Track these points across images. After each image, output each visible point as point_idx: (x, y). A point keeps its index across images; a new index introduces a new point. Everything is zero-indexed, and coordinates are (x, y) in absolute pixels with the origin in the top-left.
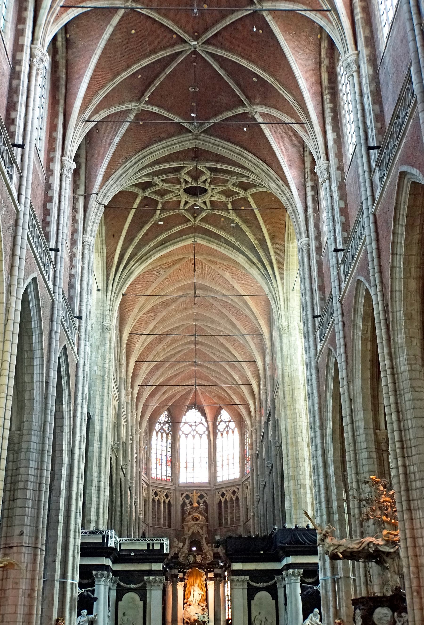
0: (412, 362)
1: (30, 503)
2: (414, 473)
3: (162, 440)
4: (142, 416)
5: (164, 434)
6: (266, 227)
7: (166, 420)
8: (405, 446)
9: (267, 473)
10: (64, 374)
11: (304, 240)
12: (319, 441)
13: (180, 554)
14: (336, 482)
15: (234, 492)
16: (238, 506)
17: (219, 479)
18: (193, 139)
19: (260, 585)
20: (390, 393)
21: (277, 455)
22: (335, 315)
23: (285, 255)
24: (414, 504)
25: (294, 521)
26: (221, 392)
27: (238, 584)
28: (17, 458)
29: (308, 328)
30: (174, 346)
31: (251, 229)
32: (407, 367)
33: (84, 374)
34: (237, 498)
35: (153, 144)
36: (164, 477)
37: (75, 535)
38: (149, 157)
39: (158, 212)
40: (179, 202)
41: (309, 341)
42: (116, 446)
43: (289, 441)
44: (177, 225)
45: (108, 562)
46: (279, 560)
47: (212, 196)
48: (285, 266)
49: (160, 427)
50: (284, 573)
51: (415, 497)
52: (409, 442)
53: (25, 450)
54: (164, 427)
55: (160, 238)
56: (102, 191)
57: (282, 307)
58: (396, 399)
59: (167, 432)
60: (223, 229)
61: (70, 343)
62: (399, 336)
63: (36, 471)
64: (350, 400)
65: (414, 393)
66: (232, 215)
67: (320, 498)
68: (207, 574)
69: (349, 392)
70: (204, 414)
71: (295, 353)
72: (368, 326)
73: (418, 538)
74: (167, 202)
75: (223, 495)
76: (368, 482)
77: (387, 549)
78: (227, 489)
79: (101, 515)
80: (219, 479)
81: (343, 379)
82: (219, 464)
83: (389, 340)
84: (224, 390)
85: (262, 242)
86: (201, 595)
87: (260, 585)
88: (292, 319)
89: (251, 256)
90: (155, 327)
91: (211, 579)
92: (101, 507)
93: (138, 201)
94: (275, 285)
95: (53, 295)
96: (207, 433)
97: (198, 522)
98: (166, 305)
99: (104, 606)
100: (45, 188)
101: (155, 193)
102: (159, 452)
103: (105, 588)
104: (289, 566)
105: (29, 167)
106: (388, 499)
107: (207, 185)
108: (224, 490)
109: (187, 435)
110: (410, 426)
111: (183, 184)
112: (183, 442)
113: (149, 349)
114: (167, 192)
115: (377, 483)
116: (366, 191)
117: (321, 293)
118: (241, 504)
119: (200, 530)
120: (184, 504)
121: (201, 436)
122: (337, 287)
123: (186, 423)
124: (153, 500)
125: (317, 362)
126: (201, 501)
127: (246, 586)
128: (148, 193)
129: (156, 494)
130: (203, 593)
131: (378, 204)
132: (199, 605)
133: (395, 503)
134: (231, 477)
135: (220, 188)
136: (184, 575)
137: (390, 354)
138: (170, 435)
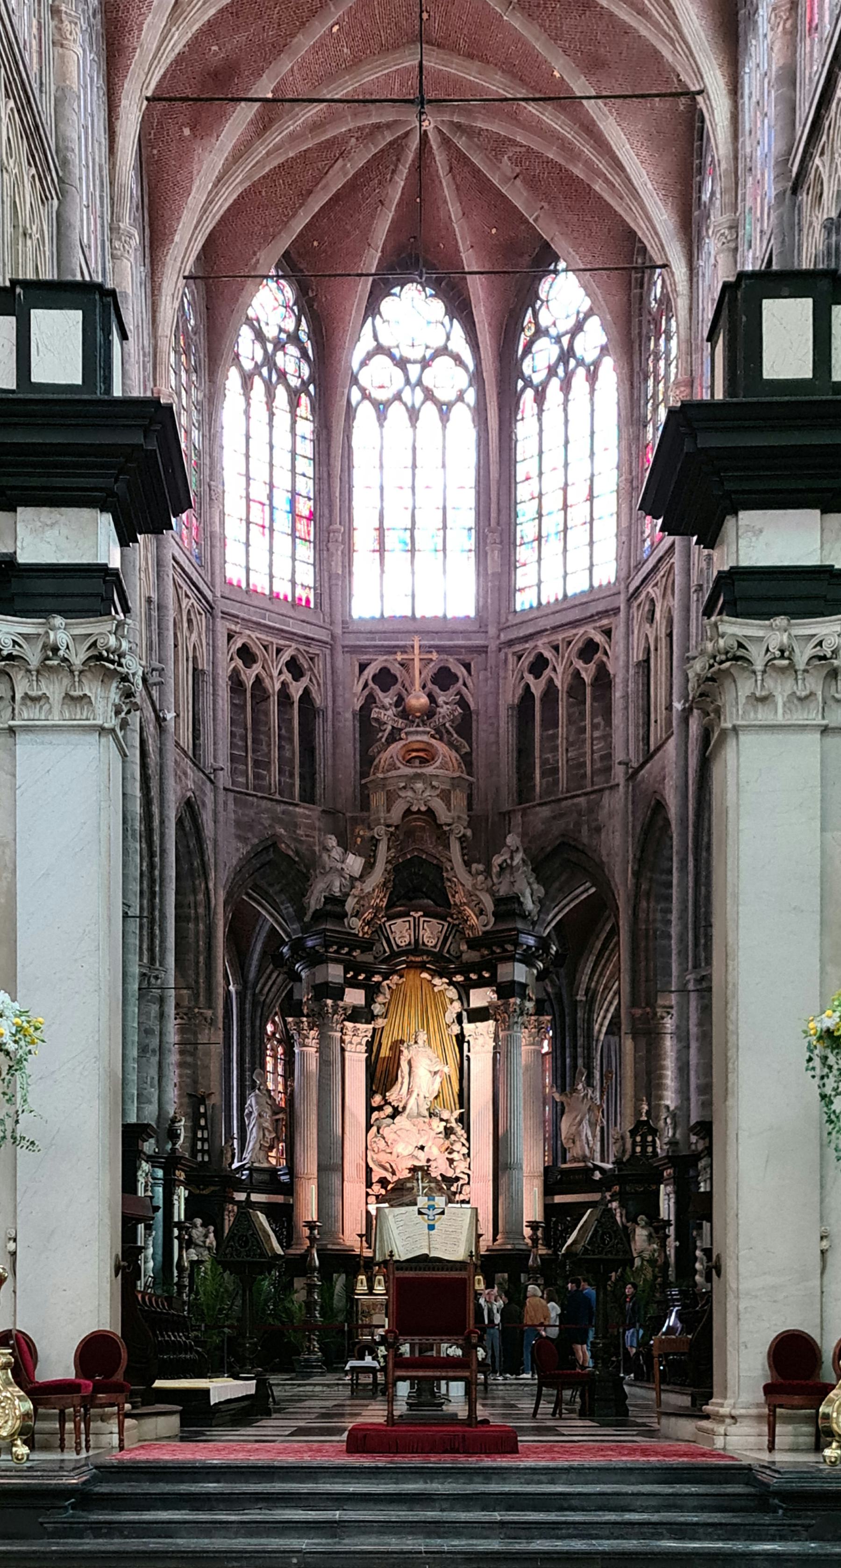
3: (272, 415)
15: (589, 650)
16: (607, 713)
34: (603, 679)
54: (280, 358)
59: (294, 382)
68: (464, 997)
78: (559, 637)
86: (438, 1079)
96: (471, 396)
102: (260, 472)
120: (371, 699)
121: (444, 410)
130: (446, 1069)
132: (431, 1115)
134: (578, 585)
138: (304, 400)
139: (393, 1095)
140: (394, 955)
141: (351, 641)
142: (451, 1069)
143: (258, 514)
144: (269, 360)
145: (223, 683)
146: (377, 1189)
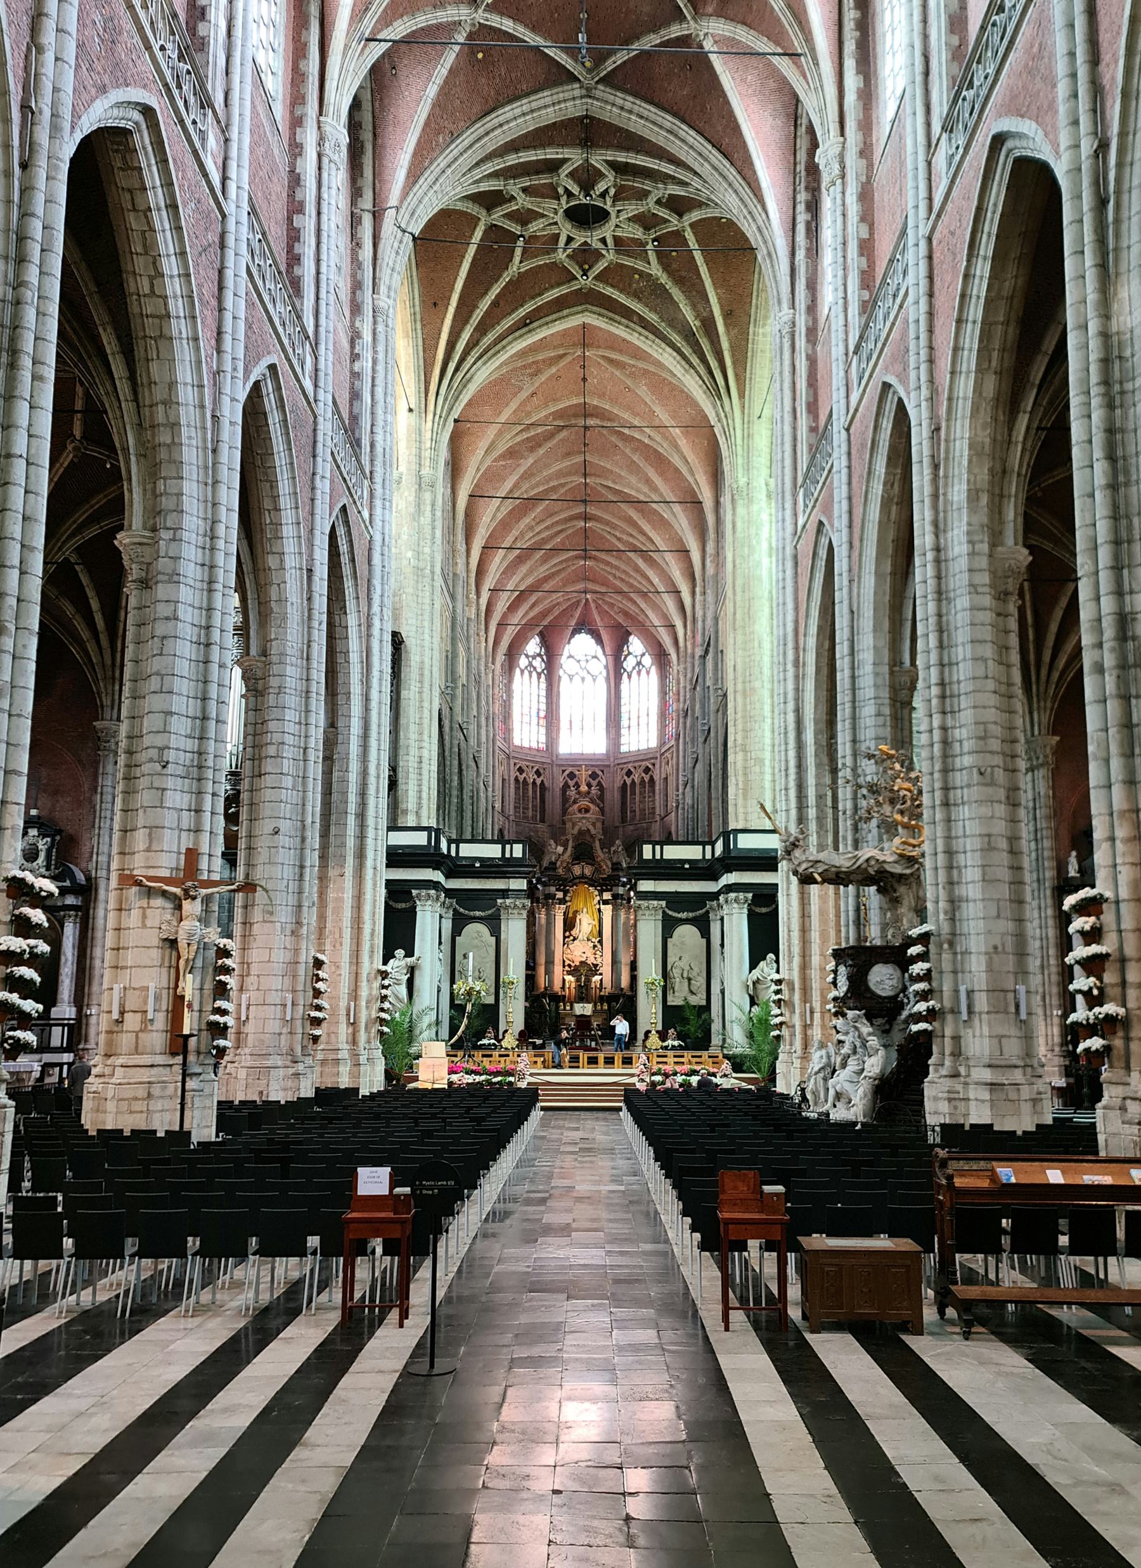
0: (976, 538)
1: (288, 782)
2: (961, 741)
4: (496, 643)
5: (534, 674)
6: (717, 294)
7: (538, 651)
8: (948, 693)
9: (701, 740)
10: (345, 559)
11: (786, 313)
12: (790, 686)
13: (559, 863)
14: (816, 755)
15: (647, 770)
17: (624, 749)
18: (582, 97)
19: (683, 915)
20: (930, 597)
21: (718, 711)
22: (835, 455)
23: (750, 349)
24: (955, 795)
25: (741, 817)
26: (629, 604)
27: (647, 913)
28: (263, 704)
29: (783, 484)
30: (548, 522)
31: (688, 298)
32: (965, 548)
33: (383, 561)
34: (652, 779)
35: (503, 105)
36: (534, 745)
37: (377, 835)
38: (496, 133)
39: (517, 258)
40: (556, 237)
41: (784, 509)
42: (449, 691)
43: (740, 687)
44: (552, 287)
45: (437, 876)
46: (715, 878)
47: (617, 226)
48: (748, 372)
49: (527, 663)
50: (721, 898)
51: (958, 784)
52: (955, 686)
53: (277, 691)
55: (522, 312)
56: (406, 204)
57: (739, 448)
58: (939, 607)
60: (637, 295)
61: (355, 502)
62: (956, 488)
63: (297, 726)
64: (852, 612)
65: (974, 596)
66: (655, 269)
67: (787, 783)
68: (601, 895)
69: (850, 599)
70: (599, 640)
71: (757, 534)
72: (895, 475)
73: (957, 852)
74: (533, 238)
75: (629, 773)
76: (874, 756)
77: (898, 869)
78: (636, 764)
79: (425, 802)
80: (624, 749)
81: (841, 575)
82: (624, 723)
83: (935, 496)
84: (635, 603)
85: (708, 325)
87: (683, 915)
88: (755, 472)
89: (687, 351)
90: (516, 486)
91: (606, 902)
92: (425, 789)
93: (478, 234)
94: (727, 408)
95: (313, 405)
96: (604, 673)
97: (587, 815)
98: (534, 444)
99: (432, 944)
100: (289, 182)
101: (509, 216)
102: (526, 704)
103: (433, 917)
104: (729, 888)
105: (242, 120)
106: (907, 785)
107: (609, 201)
108: (630, 766)
109: (571, 677)
110: (960, 657)
111: (564, 200)
112: (566, 689)
113: (505, 525)
114: (535, 215)
115: (891, 757)
116: (917, 188)
117: (811, 417)
118: (657, 788)
119: (591, 827)
120: (566, 786)
122: (843, 401)
123: (570, 656)
124: (517, 779)
125: (795, 547)
126: (594, 783)
127: (660, 917)
128: (497, 216)
129: (521, 770)
131: (939, 216)
132: (588, 940)
133: (920, 792)
134: (643, 746)
135: (632, 208)
136: (565, 895)
137: (935, 524)
138: (543, 676)
139: (573, 932)
140: (574, 879)
141: (560, 763)
142: (596, 923)
143: (526, 719)
144: (530, 664)
145: (512, 779)
146: (567, 968)
